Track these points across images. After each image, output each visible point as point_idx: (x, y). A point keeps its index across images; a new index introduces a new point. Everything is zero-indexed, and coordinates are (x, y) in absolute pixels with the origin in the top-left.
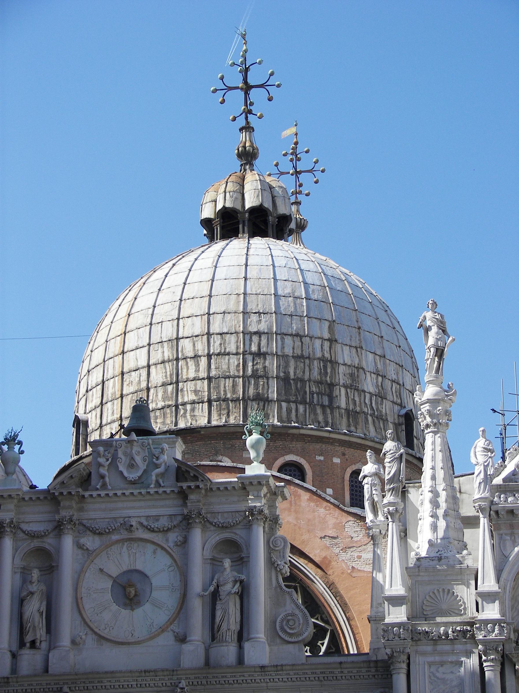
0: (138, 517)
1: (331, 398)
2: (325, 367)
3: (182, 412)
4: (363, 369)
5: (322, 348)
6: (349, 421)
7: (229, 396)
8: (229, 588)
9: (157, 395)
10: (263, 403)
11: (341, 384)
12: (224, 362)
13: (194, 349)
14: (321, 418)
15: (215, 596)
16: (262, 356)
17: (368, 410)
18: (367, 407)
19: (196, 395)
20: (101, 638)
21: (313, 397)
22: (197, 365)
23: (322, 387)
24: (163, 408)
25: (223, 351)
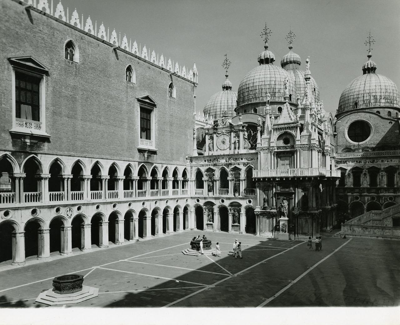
8: (237, 142)
14: (273, 99)
15: (235, 142)
20: (220, 150)
23: (273, 93)
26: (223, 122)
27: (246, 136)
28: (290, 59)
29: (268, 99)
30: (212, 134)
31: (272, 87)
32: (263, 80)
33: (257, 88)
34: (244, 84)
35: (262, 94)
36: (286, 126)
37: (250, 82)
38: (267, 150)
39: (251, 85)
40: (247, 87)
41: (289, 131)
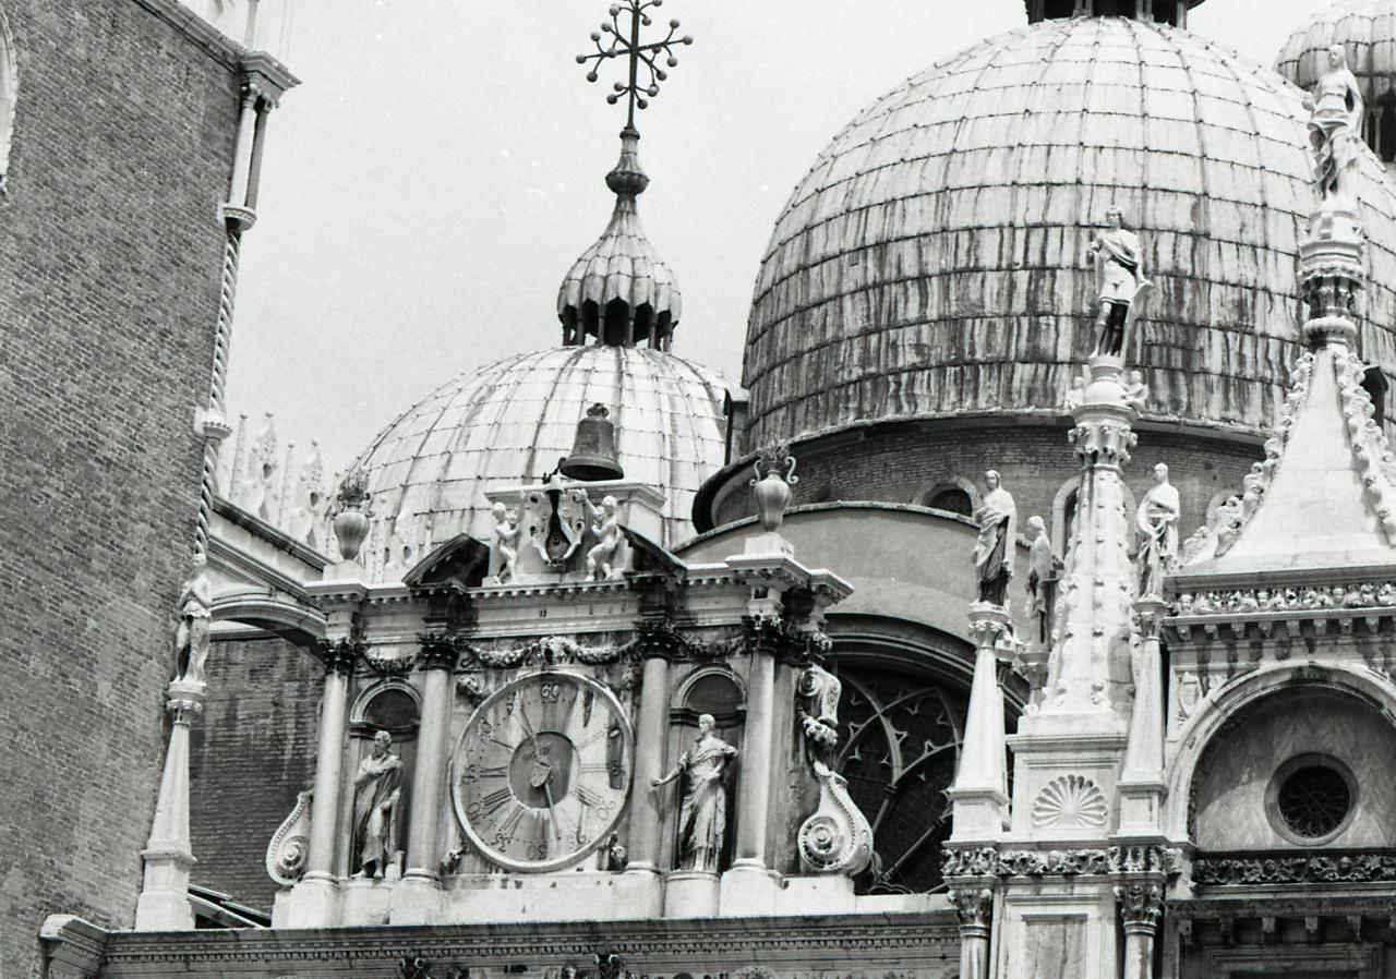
0: (562, 635)
1: (1188, 350)
2: (1179, 290)
3: (893, 387)
4: (1265, 290)
5: (1174, 251)
6: (1226, 398)
7: (979, 356)
8: (706, 773)
9: (851, 355)
10: (1044, 367)
11: (1213, 323)
12: (974, 283)
13: (920, 262)
16: (1048, 273)
17: (1273, 374)
18: (1271, 368)
19: (918, 354)
21: (1150, 355)
22: (924, 294)
23: (1172, 333)
24: (860, 380)
25: (972, 265)
26: (555, 524)
27: (830, 713)
28: (1370, 54)
29: (1108, 293)
30: (399, 670)
31: (1166, 261)
32: (1063, 170)
33: (988, 258)
34: (831, 204)
35: (1035, 330)
36: (1316, 604)
37: (909, 180)
38: (1069, 877)
39: (919, 218)
40: (870, 240)
41: (1357, 667)
